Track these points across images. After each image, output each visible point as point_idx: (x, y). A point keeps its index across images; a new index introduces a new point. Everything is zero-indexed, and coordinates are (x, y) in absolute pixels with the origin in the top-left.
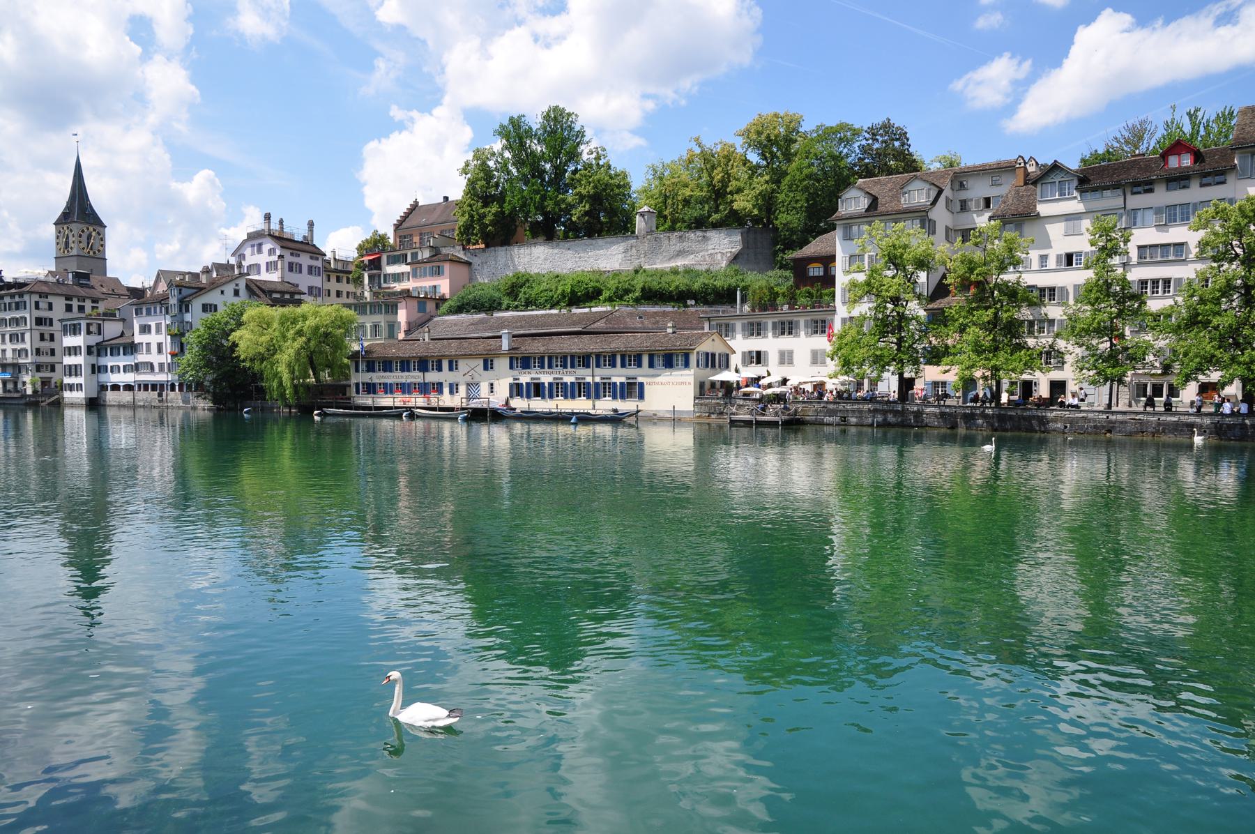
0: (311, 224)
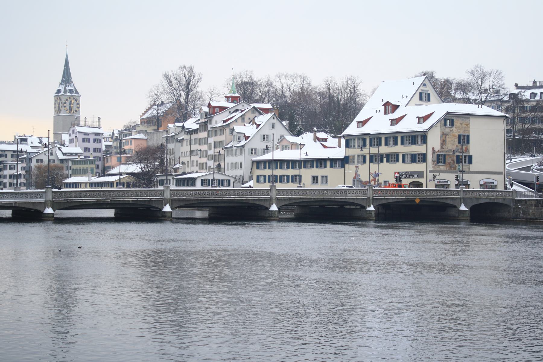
0: (99, 118)
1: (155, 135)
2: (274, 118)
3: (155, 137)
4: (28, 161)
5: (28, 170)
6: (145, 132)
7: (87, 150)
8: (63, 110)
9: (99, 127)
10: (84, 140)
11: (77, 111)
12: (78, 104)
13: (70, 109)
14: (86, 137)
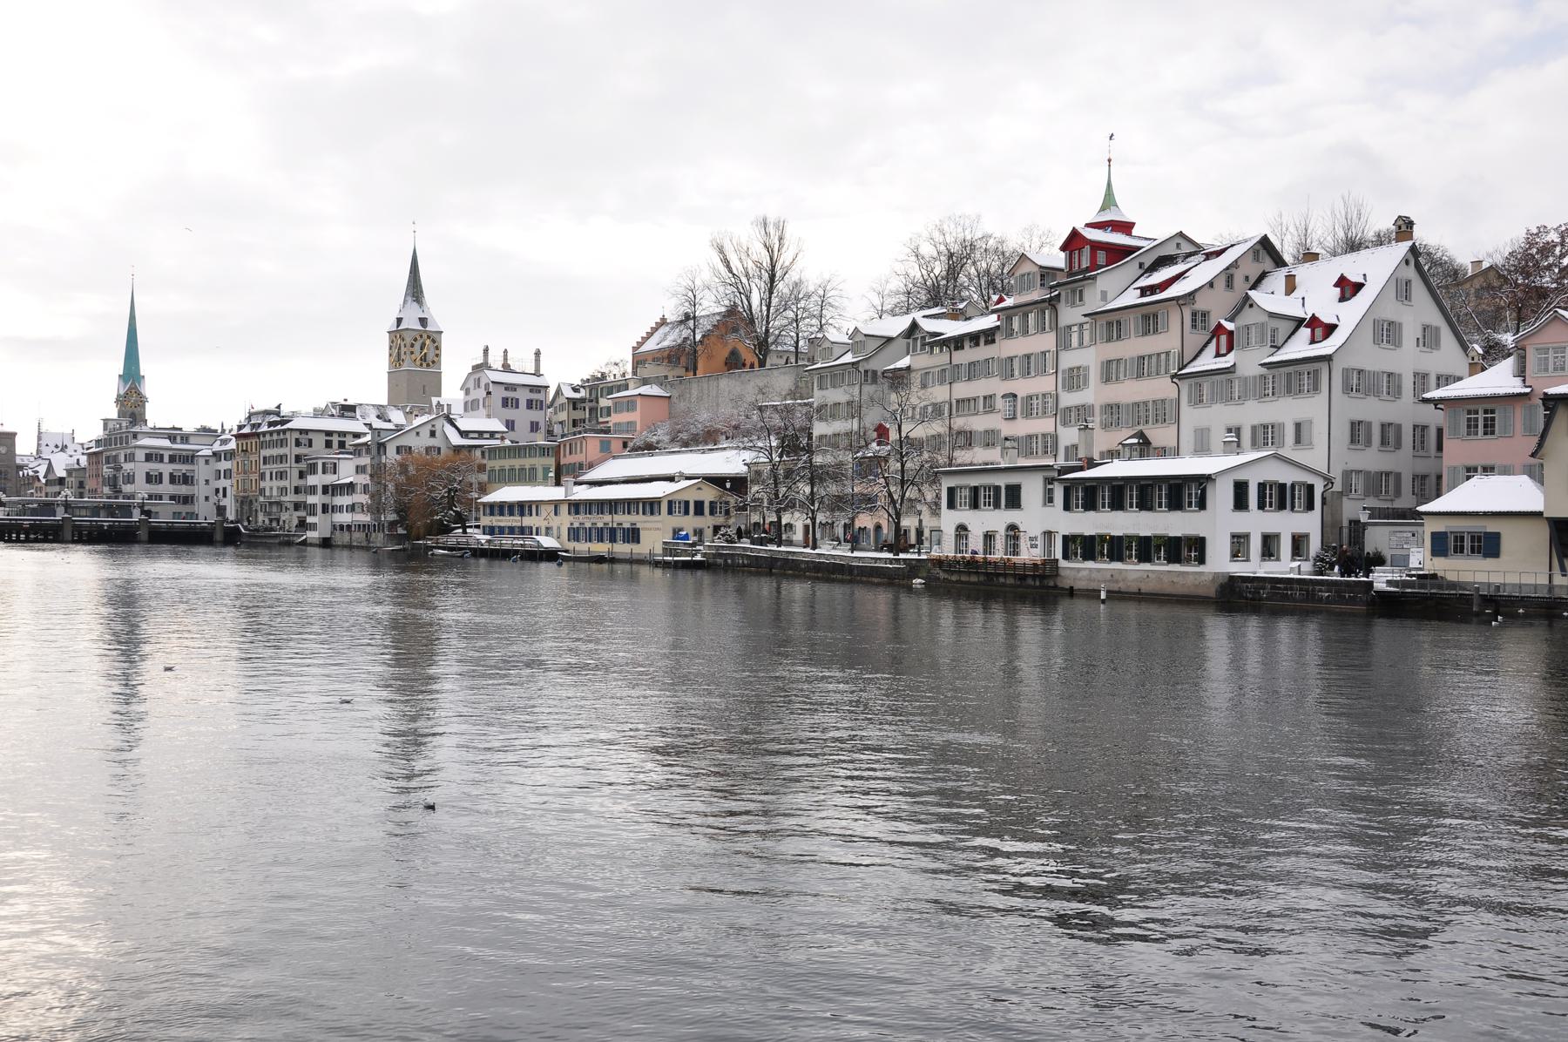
0: (538, 354)
1: (694, 386)
2: (1407, 262)
3: (695, 393)
4: (374, 450)
5: (378, 472)
6: (661, 381)
7: (510, 425)
8: (407, 358)
9: (537, 374)
10: (505, 402)
11: (436, 362)
12: (437, 348)
13: (424, 359)
14: (510, 394)
